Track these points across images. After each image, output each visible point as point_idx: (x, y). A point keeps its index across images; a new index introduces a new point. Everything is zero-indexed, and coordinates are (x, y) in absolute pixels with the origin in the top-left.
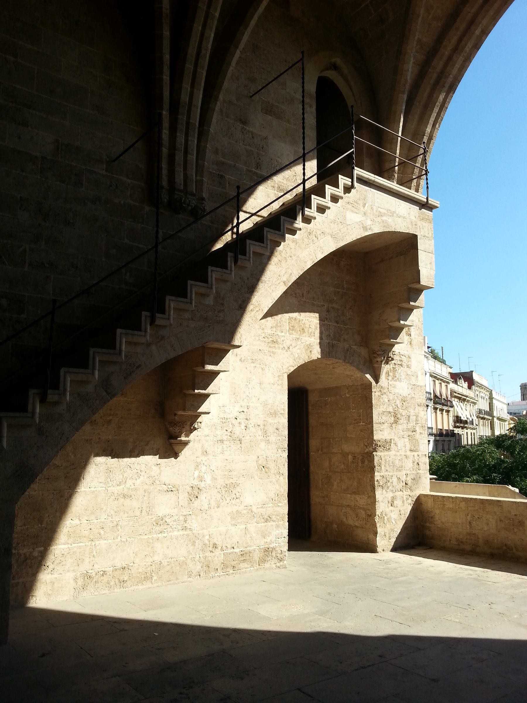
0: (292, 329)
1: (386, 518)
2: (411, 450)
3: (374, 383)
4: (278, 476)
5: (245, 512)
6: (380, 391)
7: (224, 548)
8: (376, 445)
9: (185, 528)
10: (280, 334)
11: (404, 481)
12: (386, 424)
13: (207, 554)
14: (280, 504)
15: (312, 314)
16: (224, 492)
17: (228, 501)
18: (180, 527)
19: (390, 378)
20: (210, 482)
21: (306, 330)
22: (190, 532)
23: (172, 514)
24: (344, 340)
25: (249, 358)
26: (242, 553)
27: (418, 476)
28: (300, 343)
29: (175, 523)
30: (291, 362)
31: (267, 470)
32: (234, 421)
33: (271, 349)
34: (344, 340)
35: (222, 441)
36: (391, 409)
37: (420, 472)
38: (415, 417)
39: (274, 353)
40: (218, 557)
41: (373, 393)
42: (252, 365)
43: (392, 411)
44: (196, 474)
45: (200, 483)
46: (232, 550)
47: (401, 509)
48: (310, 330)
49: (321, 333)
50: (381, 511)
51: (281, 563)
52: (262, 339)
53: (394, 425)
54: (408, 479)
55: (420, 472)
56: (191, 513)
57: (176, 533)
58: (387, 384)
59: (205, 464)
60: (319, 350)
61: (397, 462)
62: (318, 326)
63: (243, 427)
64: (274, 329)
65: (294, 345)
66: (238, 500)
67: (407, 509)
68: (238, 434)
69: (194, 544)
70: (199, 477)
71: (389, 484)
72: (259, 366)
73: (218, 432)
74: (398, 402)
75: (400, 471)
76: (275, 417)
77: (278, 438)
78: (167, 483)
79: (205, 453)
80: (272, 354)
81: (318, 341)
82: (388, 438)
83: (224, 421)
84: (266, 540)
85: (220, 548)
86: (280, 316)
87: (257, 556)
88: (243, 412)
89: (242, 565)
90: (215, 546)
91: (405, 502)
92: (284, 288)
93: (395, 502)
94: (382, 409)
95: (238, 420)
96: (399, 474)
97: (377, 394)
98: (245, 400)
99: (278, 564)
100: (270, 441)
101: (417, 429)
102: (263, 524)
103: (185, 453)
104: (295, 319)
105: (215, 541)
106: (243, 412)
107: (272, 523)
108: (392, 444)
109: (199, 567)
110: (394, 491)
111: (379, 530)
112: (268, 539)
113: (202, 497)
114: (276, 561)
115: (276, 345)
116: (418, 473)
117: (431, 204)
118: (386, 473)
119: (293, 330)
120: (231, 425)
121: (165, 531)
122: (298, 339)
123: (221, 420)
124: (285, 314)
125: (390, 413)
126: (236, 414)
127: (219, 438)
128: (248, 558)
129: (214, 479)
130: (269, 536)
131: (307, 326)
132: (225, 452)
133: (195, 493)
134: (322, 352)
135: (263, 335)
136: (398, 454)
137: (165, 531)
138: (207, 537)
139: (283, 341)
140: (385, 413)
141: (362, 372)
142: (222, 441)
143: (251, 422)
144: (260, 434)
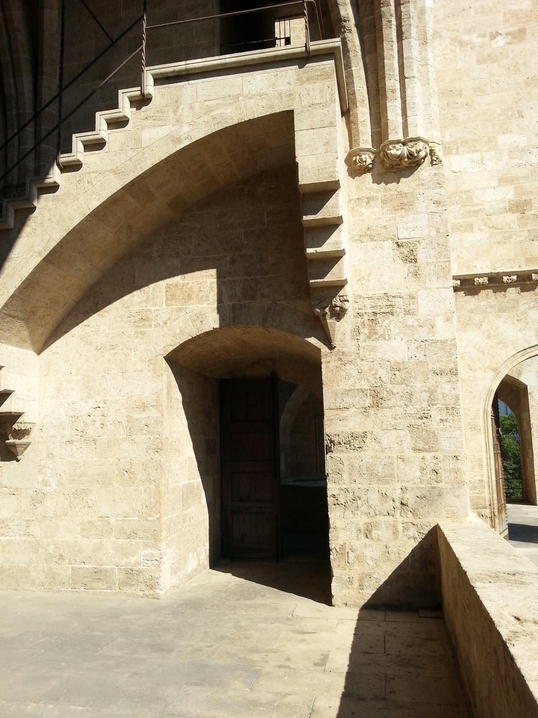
0: (171, 298)
1: (351, 555)
2: (415, 449)
3: (324, 349)
4: (147, 484)
5: (99, 523)
6: (340, 359)
7: (73, 562)
8: (332, 442)
9: (28, 534)
10: (152, 309)
11: (396, 498)
12: (353, 410)
13: (51, 565)
14: (151, 519)
15: (204, 273)
16: (72, 500)
17: (77, 510)
18: (22, 532)
19: (362, 337)
20: (56, 488)
21: (194, 296)
22: (33, 539)
23: (13, 518)
24: (263, 295)
25: (107, 344)
26: (95, 570)
27: (436, 492)
28: (184, 313)
29: (16, 527)
30: (169, 341)
31: (131, 475)
32: (86, 419)
33: (139, 330)
34: (263, 295)
35: (71, 442)
36: (365, 385)
37: (441, 485)
38: (426, 395)
39: (142, 333)
40: (65, 570)
41: (323, 366)
42: (112, 352)
43: (368, 388)
44: (40, 478)
45: (45, 488)
46: (83, 565)
47: (390, 545)
48: (201, 294)
49: (220, 294)
50: (342, 543)
51: (152, 592)
52: (125, 320)
53: (372, 411)
54: (407, 496)
55: (441, 485)
56: (34, 518)
57: (18, 538)
58: (353, 348)
59: (51, 467)
60: (217, 317)
61: (379, 468)
62: (215, 286)
63: (98, 424)
64: (144, 304)
65: (173, 317)
66: (91, 510)
67: (406, 546)
68: (91, 433)
69: (36, 552)
70: (43, 481)
71: (359, 503)
72: (121, 351)
73: (66, 432)
74: (382, 373)
75: (387, 482)
76: (144, 410)
77: (148, 436)
78: (8, 485)
79: (51, 455)
80: (139, 335)
81: (215, 305)
82: (359, 430)
83: (73, 419)
84: (128, 560)
85: (67, 561)
86: (152, 286)
87: (118, 576)
88: (99, 407)
89: (95, 585)
90: (61, 557)
91: (400, 533)
92: (39, 259)
93: (374, 532)
94: (343, 386)
95: (92, 417)
96: (384, 488)
97: (332, 364)
98: (102, 394)
99: (147, 592)
100: (136, 440)
101: (434, 413)
102: (124, 540)
103: (25, 457)
104: (176, 285)
105: (61, 552)
106: (99, 407)
107: (138, 540)
108: (368, 441)
109: (42, 577)
110: (373, 514)
111: (336, 571)
112: (132, 560)
113: (48, 503)
114: (143, 587)
115: (147, 323)
116: (433, 488)
117: (315, 51)
118: (353, 485)
119: (172, 299)
120: (82, 424)
121: (7, 534)
122: (180, 309)
123: (71, 419)
124: (160, 282)
125: (362, 391)
126: (88, 410)
127: (68, 438)
128: (102, 577)
129: (60, 484)
130: (133, 556)
131: (196, 290)
132: (75, 455)
133: (38, 499)
134: (222, 320)
135: (128, 314)
136: (382, 455)
137: (7, 534)
138: (52, 547)
139: (157, 316)
140: (350, 393)
141: (299, 335)
142: (71, 442)
143: (109, 418)
144: (122, 432)
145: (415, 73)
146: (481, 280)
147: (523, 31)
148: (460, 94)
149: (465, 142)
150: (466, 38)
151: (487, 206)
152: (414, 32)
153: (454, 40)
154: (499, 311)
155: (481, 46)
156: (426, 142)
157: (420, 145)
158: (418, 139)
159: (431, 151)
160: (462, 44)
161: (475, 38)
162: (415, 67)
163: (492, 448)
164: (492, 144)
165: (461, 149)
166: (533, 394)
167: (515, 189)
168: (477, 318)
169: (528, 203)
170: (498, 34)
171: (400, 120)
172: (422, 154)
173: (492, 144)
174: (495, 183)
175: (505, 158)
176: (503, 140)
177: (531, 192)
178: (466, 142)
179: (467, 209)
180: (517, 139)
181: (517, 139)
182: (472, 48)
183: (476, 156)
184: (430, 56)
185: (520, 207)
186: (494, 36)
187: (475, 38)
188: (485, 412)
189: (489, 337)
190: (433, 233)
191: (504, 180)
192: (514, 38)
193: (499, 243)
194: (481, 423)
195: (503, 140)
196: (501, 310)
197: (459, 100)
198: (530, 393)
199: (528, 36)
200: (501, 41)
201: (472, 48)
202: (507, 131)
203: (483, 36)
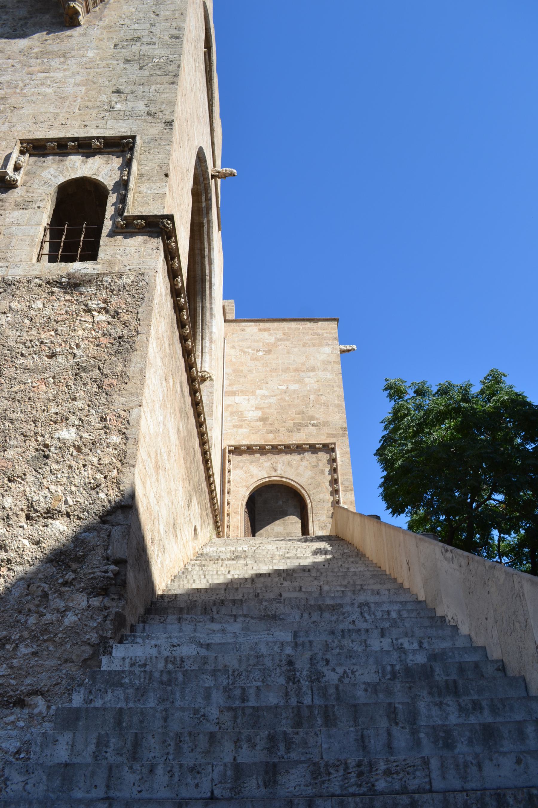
145: (207, 351)
146: (243, 448)
147: (270, 351)
148: (242, 372)
149: (242, 391)
150: (246, 350)
151: (249, 418)
152: (207, 338)
153: (241, 350)
154: (251, 462)
155: (252, 354)
156: (208, 373)
157: (206, 373)
158: (205, 371)
159: (210, 377)
160: (244, 352)
161: (250, 351)
162: (207, 349)
163: (243, 521)
164: (253, 393)
165: (240, 394)
167: (262, 412)
168: (241, 465)
169: (267, 418)
170: (260, 350)
171: (200, 365)
172: (207, 376)
173: (253, 393)
174: (254, 409)
175: (259, 399)
176: (258, 392)
177: (269, 414)
178: (243, 391)
179: (241, 419)
180: (264, 392)
181: (264, 392)
182: (249, 354)
183: (247, 397)
184: (213, 346)
185: (263, 419)
186: (258, 351)
187: (250, 351)
188: (242, 506)
189: (246, 473)
190: (208, 402)
191: (257, 408)
192: (266, 352)
193: (253, 434)
194: (240, 510)
195: (258, 392)
196: (252, 462)
197: (241, 374)
199: (272, 353)
200: (261, 353)
201: (249, 354)
202: (260, 389)
203: (254, 350)
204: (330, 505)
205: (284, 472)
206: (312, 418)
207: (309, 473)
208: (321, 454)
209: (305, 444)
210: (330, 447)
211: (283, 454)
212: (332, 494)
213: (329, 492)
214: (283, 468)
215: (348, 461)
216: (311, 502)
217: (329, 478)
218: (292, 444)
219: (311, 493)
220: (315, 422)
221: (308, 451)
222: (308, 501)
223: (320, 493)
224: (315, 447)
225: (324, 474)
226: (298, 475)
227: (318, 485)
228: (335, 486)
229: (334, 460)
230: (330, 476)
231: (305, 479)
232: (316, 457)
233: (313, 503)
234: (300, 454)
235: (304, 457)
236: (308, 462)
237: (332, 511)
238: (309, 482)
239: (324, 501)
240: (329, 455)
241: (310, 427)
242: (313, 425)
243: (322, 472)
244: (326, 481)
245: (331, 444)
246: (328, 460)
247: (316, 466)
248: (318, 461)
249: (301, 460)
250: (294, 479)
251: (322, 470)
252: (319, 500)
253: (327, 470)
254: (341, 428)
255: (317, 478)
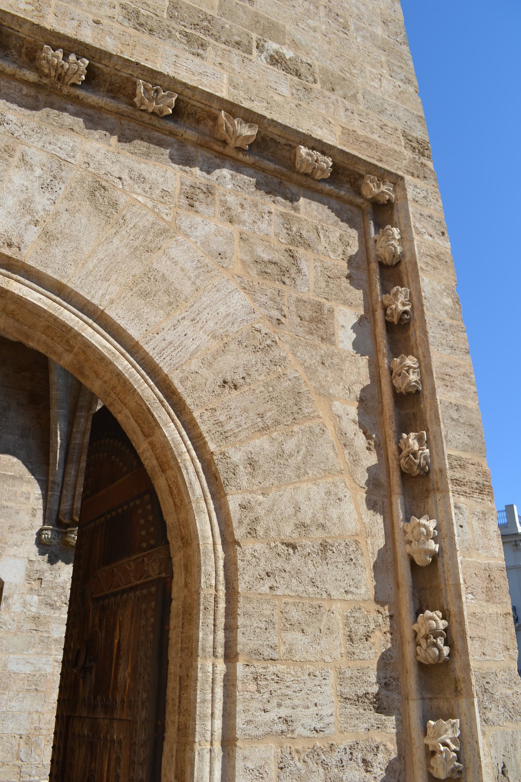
166: (10, 601)
198: (7, 598)
204: (366, 584)
205: (47, 236)
206: (271, 29)
207: (231, 303)
208: (311, 212)
209: (234, 110)
210: (373, 188)
211: (67, 119)
212: (377, 496)
213: (363, 477)
214: (41, 202)
215: (448, 301)
216: (229, 542)
217: (358, 372)
218: (152, 75)
219: (237, 456)
220: (289, 54)
221: (238, 166)
222: (205, 527)
223: (300, 474)
224: (290, 163)
225: (328, 338)
226: (149, 287)
227: (291, 407)
228: (412, 441)
229: (393, 272)
230: (363, 361)
231: (200, 340)
232: (287, 221)
233: (248, 548)
234: (185, 160)
235: (209, 191)
236: (227, 228)
237: (381, 642)
238: (231, 363)
239: (324, 547)
240: (354, 233)
241: (259, 60)
242: (276, 60)
243: (318, 321)
244: (336, 390)
245: (383, 175)
246: (351, 261)
247: (284, 272)
248: (292, 242)
249: (191, 199)
250: (114, 313)
251: (319, 307)
252: (288, 531)
253: (346, 317)
254: (405, 135)
255: (283, 350)
